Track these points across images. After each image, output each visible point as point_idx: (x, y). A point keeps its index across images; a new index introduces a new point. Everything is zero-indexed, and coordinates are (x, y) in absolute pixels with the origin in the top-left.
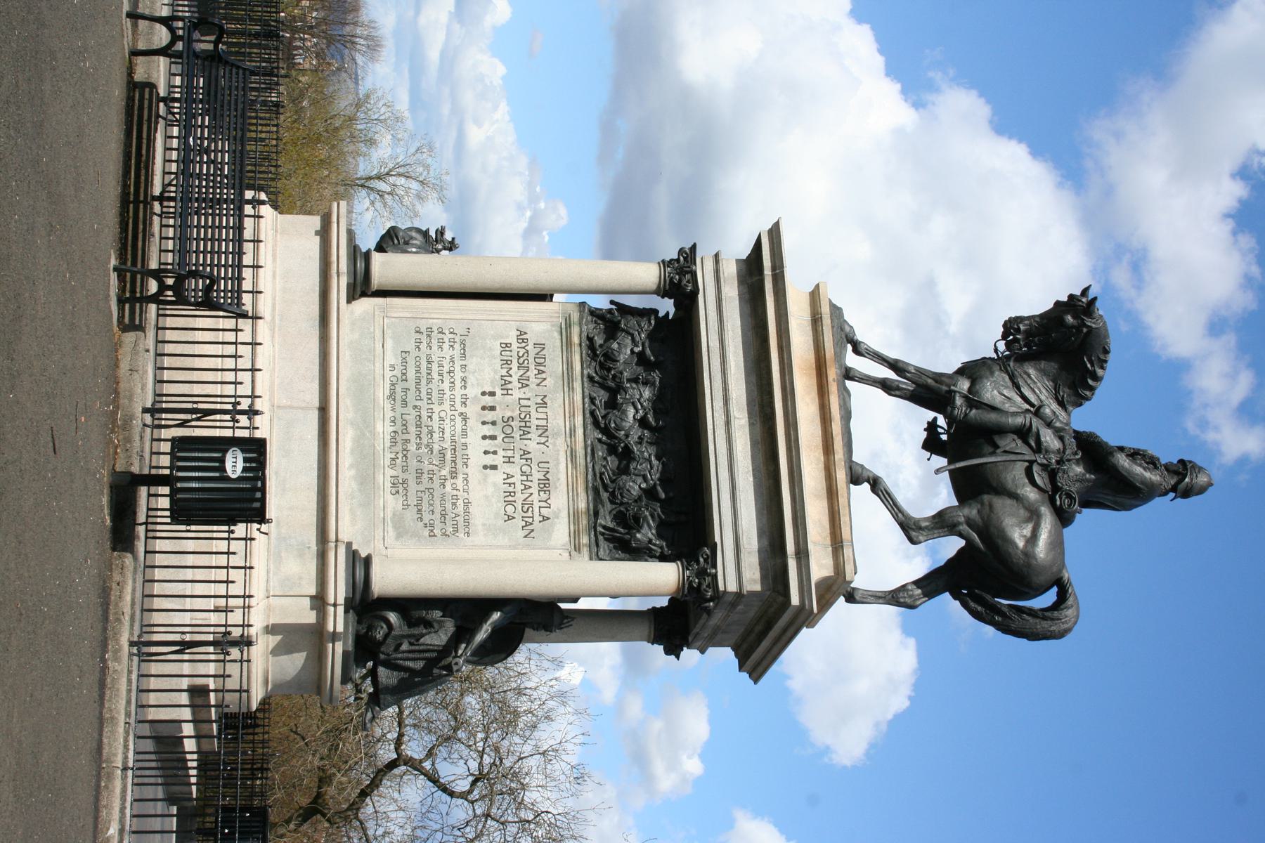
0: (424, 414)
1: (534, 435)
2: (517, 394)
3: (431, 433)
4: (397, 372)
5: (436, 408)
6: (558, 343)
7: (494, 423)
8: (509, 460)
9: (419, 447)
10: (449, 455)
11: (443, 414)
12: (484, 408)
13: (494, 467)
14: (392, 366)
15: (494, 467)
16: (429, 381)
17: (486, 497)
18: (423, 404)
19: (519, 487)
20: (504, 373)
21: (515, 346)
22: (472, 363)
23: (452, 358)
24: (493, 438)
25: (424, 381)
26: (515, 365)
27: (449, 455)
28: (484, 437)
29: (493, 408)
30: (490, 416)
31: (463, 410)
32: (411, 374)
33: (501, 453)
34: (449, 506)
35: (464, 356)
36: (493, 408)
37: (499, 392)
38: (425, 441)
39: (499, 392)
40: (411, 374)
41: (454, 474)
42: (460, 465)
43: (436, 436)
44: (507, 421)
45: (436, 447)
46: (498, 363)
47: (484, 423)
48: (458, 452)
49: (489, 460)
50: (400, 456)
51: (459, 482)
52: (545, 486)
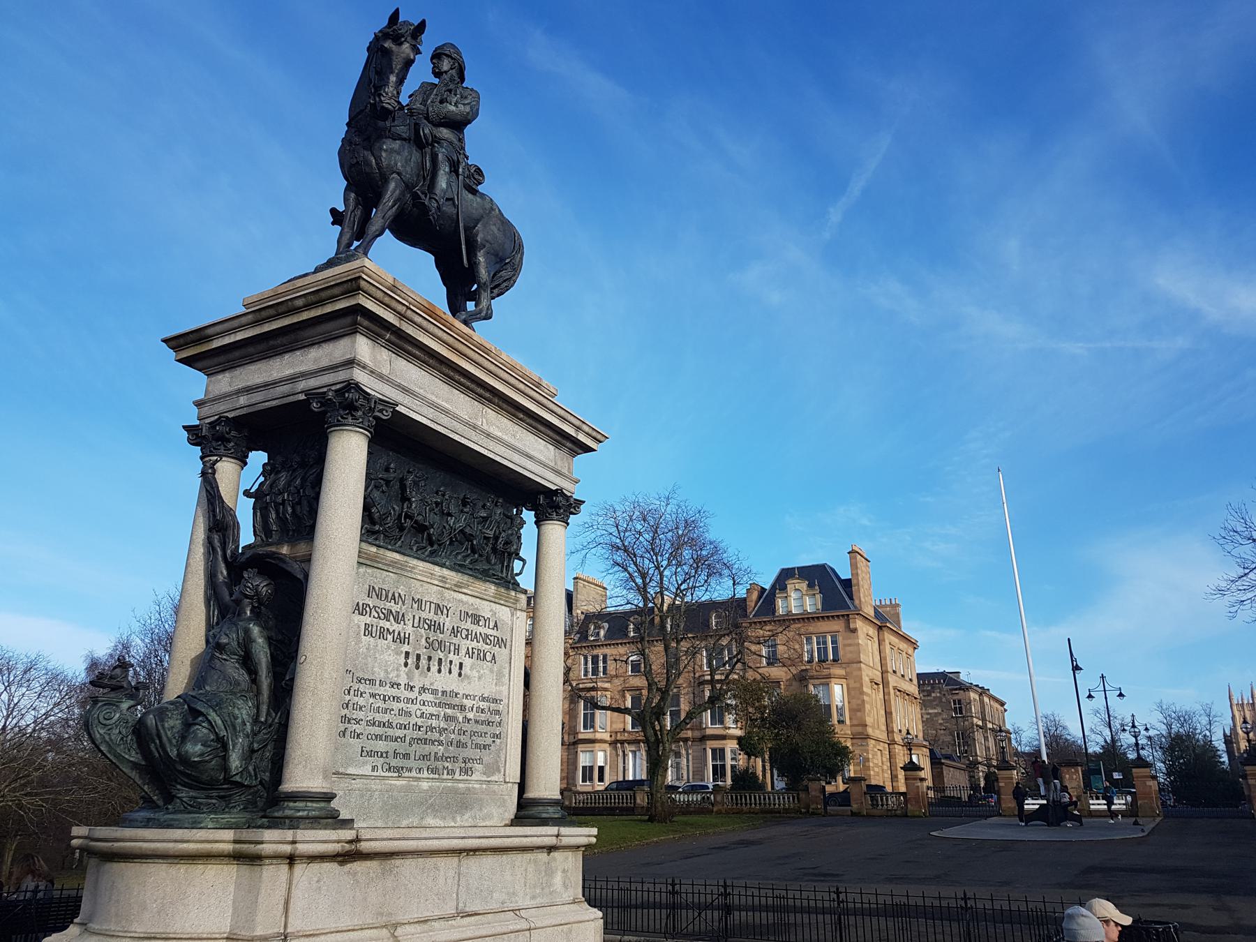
0: (416, 734)
1: (441, 619)
2: (409, 629)
3: (432, 729)
5: (413, 720)
6: (370, 570)
7: (430, 658)
8: (457, 650)
9: (441, 743)
10: (449, 711)
11: (419, 713)
12: (417, 668)
13: (461, 664)
15: (461, 664)
18: (410, 734)
19: (474, 644)
20: (390, 637)
21: (368, 620)
22: (380, 674)
23: (373, 695)
25: (390, 732)
26: (387, 625)
27: (449, 711)
28: (439, 671)
29: (418, 657)
30: (424, 662)
31: (416, 690)
32: (381, 746)
33: (451, 656)
34: (483, 717)
35: (372, 682)
36: (418, 657)
37: (406, 648)
39: (406, 648)
40: (381, 746)
41: (462, 708)
42: (456, 701)
43: (434, 723)
44: (430, 645)
45: (443, 725)
46: (381, 642)
47: (429, 669)
48: (447, 699)
49: (455, 670)
50: (446, 764)
52: (476, 619)
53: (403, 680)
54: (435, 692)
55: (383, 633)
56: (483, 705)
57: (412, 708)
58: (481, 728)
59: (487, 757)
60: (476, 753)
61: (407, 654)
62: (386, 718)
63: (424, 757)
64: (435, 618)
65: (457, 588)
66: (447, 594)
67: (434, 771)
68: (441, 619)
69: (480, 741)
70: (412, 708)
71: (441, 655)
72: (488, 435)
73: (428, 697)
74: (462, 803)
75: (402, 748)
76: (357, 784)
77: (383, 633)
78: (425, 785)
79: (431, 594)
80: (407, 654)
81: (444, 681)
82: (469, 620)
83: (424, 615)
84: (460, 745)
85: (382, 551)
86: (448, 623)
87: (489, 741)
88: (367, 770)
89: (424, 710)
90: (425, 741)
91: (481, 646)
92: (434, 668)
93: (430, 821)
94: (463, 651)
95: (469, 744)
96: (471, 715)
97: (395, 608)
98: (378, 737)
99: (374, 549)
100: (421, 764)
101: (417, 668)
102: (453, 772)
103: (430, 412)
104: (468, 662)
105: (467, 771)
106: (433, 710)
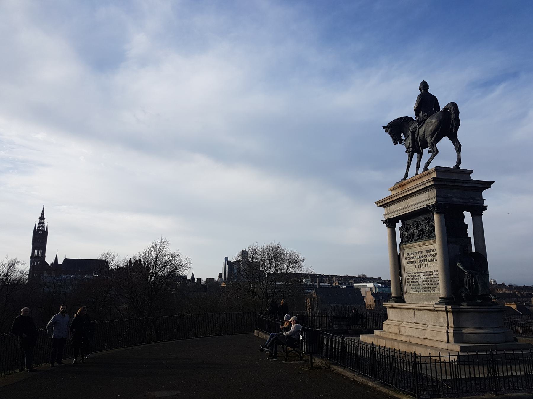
2: (415, 260)
8: (426, 261)
18: (420, 283)
26: (411, 260)
32: (414, 286)
40: (414, 286)
41: (430, 275)
42: (428, 274)
48: (426, 274)
49: (427, 266)
51: (431, 273)
52: (430, 251)
54: (423, 272)
55: (411, 262)
58: (435, 279)
60: (435, 286)
65: (424, 245)
66: (422, 248)
67: (426, 291)
75: (418, 286)
77: (411, 262)
79: (418, 249)
84: (431, 284)
86: (423, 255)
89: (421, 278)
90: (423, 284)
91: (432, 257)
93: (425, 303)
97: (411, 256)
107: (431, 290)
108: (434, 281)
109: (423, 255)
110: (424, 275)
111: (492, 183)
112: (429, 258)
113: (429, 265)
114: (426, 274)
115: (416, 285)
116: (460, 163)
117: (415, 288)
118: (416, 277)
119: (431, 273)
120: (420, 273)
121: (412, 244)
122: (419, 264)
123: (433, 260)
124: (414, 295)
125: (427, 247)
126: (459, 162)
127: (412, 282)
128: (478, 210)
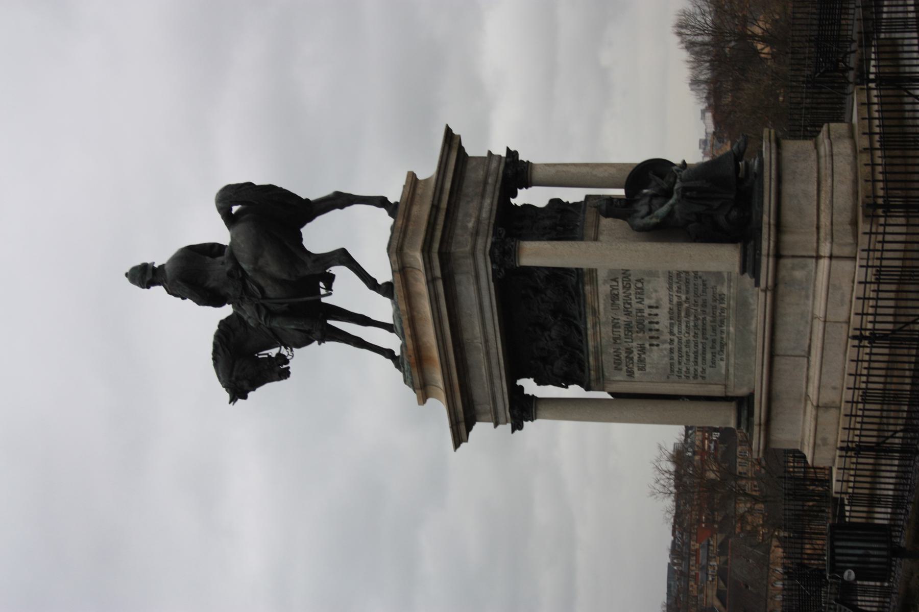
0: (700, 336)
1: (622, 323)
2: (635, 344)
3: (696, 326)
4: (718, 357)
5: (692, 338)
6: (605, 370)
7: (651, 330)
8: (641, 311)
9: (704, 319)
10: (683, 314)
12: (658, 338)
13: (650, 307)
14: (722, 360)
15: (650, 307)
16: (696, 353)
17: (656, 291)
18: (700, 340)
19: (633, 297)
21: (635, 369)
22: (666, 360)
23: (680, 363)
24: (651, 323)
26: (636, 358)
27: (683, 314)
28: (657, 323)
29: (651, 338)
30: (654, 334)
32: (709, 356)
33: (646, 314)
34: (683, 287)
35: (672, 365)
36: (651, 338)
37: (647, 346)
38: (700, 322)
39: (647, 346)
40: (709, 356)
41: (679, 304)
42: (675, 309)
43: (692, 324)
44: (642, 330)
45: (692, 318)
46: (648, 360)
47: (658, 330)
48: (675, 315)
49: (654, 311)
50: (718, 314)
51: (675, 300)
52: (614, 297)
53: (668, 346)
54: (672, 325)
55: (641, 360)
56: (675, 288)
57: (684, 339)
58: (691, 286)
59: (711, 282)
60: (710, 291)
61: (651, 345)
62: (692, 355)
63: (714, 330)
64: (623, 327)
65: (595, 313)
67: (722, 322)
68: (622, 323)
69: (701, 288)
70: (684, 339)
71: (646, 322)
72: (486, 341)
73: (676, 330)
74: (743, 305)
75: (709, 344)
76: (731, 370)
77: (641, 360)
78: (732, 329)
79: (606, 331)
80: (651, 345)
81: (664, 320)
82: (617, 302)
83: (623, 335)
84: (704, 304)
85: (592, 368)
86: (623, 319)
87: (700, 282)
88: (723, 364)
90: (704, 329)
91: (632, 291)
92: (656, 326)
94: (640, 306)
95: (703, 297)
96: (684, 297)
97: (623, 355)
98: (704, 359)
99: (592, 373)
100: (718, 332)
101: (658, 338)
102: (722, 309)
103: (497, 382)
104: (647, 302)
105: (721, 298)
106: (683, 327)
107: (719, 306)
108: (696, 295)
109: (623, 319)
110: (680, 322)
111: (449, 132)
112: (634, 301)
113: (652, 302)
114: (676, 315)
115: (704, 348)
116: (385, 199)
117: (714, 355)
118: (684, 349)
119: (675, 300)
120: (671, 333)
121: (591, 348)
122: (647, 334)
123: (640, 292)
124: (732, 361)
125: (602, 305)
126: (381, 202)
127: (696, 363)
128: (515, 171)
